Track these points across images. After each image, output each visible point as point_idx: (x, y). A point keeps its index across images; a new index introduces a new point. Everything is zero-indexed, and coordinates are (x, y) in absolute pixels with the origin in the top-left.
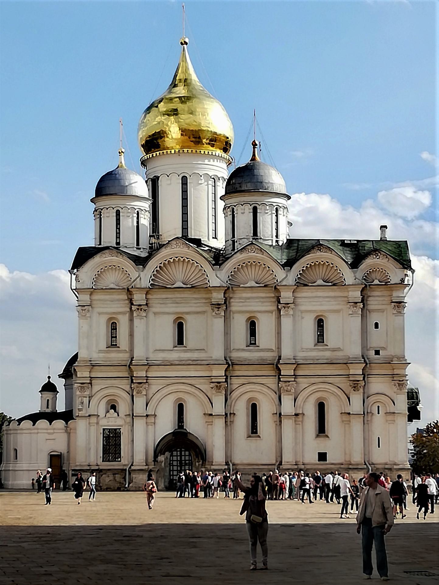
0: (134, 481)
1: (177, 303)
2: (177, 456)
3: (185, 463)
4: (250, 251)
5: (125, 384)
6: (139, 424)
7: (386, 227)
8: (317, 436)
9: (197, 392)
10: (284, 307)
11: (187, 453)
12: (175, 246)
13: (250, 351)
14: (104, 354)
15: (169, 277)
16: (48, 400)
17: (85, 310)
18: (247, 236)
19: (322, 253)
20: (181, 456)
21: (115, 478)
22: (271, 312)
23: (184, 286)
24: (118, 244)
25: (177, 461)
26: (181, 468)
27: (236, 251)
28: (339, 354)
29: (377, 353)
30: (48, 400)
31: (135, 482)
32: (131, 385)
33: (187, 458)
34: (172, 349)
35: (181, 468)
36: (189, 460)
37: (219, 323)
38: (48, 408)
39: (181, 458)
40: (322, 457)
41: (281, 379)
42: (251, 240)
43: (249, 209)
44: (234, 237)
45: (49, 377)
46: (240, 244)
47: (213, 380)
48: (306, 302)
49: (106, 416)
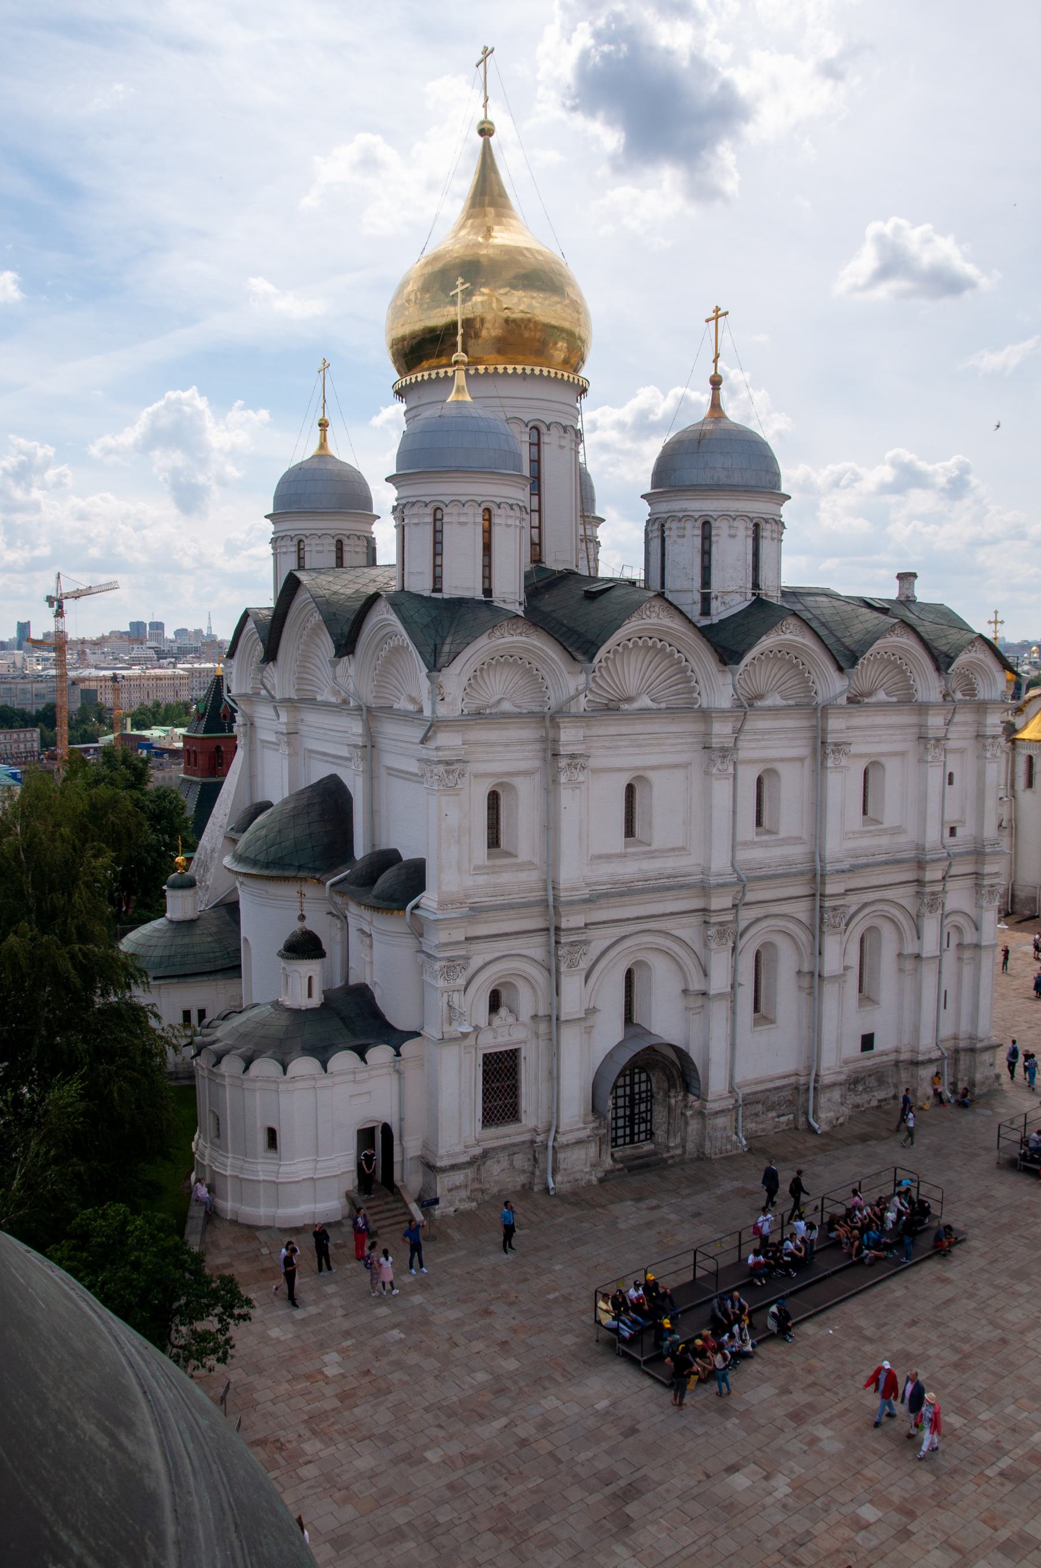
0: (562, 1166)
1: (640, 746)
2: (625, 1086)
3: (640, 1098)
4: (784, 628)
5: (535, 948)
6: (570, 1040)
7: (914, 575)
8: (860, 1005)
9: (676, 948)
10: (833, 752)
11: (644, 1077)
12: (648, 613)
13: (765, 845)
14: (486, 877)
15: (614, 682)
16: (310, 978)
17: (453, 771)
18: (740, 587)
19: (895, 639)
20: (632, 1085)
21: (512, 1164)
22: (801, 760)
23: (654, 706)
24: (488, 592)
25: (625, 1096)
26: (632, 1111)
27: (715, 620)
28: (902, 839)
29: (953, 831)
30: (310, 978)
31: (565, 1169)
32: (557, 949)
33: (643, 1087)
34: (623, 851)
35: (632, 1111)
36: (646, 1091)
37: (721, 790)
38: (310, 995)
39: (632, 1089)
40: (867, 1042)
41: (827, 904)
42: (749, 596)
43: (746, 528)
44: (706, 582)
45: (302, 918)
46: (724, 603)
47: (713, 920)
48: (859, 736)
49: (490, 1024)
